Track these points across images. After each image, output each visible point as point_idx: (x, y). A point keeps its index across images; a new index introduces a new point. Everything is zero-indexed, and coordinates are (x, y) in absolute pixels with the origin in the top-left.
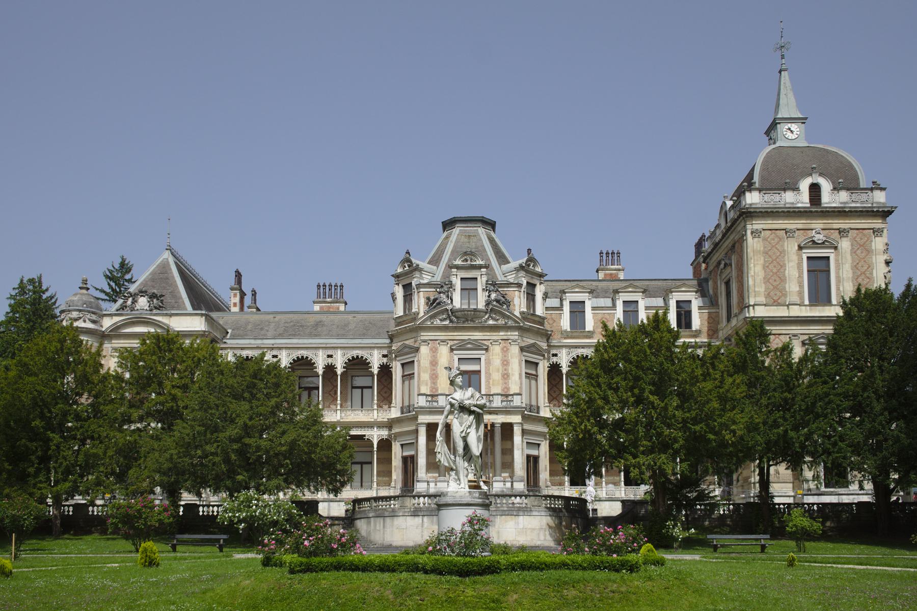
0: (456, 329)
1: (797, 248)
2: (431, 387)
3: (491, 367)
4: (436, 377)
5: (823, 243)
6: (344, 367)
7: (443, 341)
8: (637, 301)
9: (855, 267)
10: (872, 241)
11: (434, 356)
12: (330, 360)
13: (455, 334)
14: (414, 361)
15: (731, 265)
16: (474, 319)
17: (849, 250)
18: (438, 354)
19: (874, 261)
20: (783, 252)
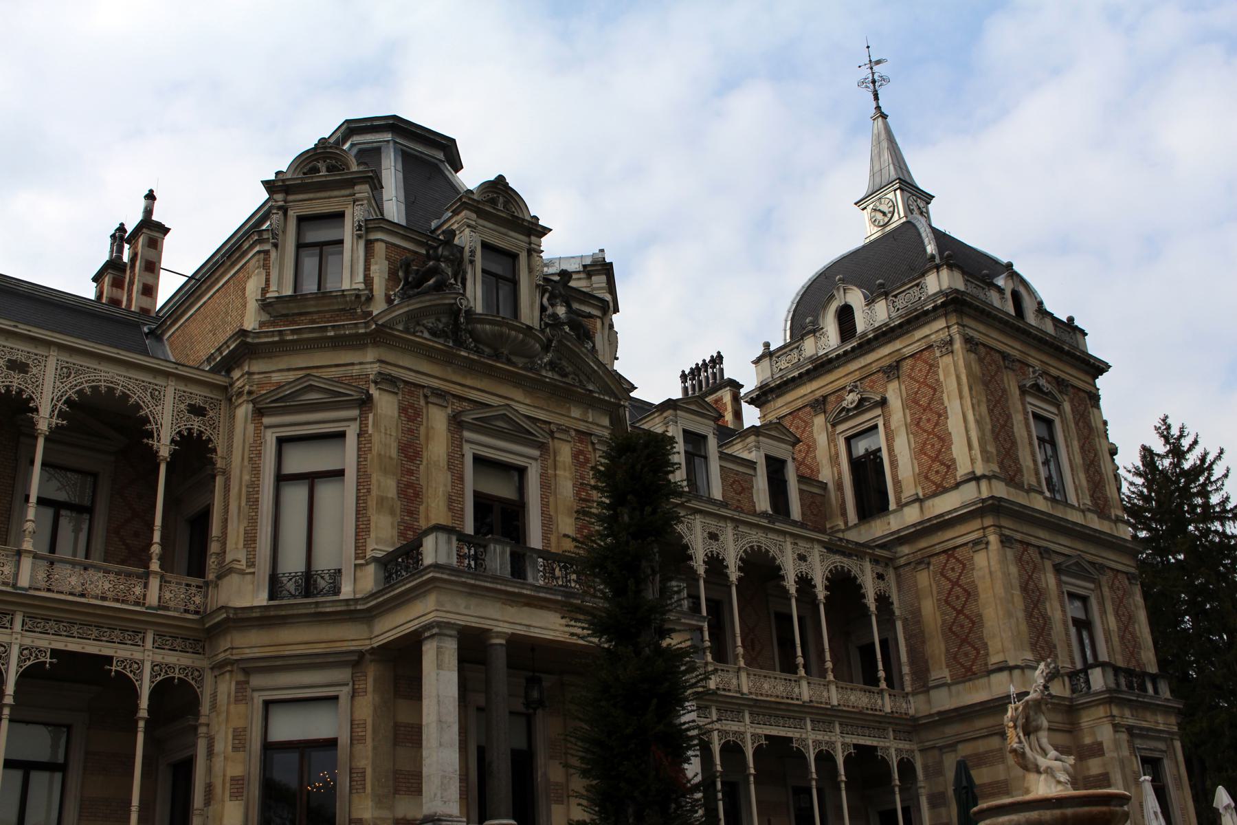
0: (471, 368)
1: (1017, 392)
2: (403, 521)
3: (552, 499)
4: (417, 495)
5: (1046, 394)
6: (61, 415)
7: (440, 394)
8: (705, 438)
9: (1082, 448)
10: (1089, 412)
11: (410, 431)
12: (16, 380)
13: (469, 382)
14: (342, 435)
15: (883, 403)
16: (514, 359)
17: (1071, 417)
18: (422, 430)
19: (1098, 447)
20: (1004, 391)
